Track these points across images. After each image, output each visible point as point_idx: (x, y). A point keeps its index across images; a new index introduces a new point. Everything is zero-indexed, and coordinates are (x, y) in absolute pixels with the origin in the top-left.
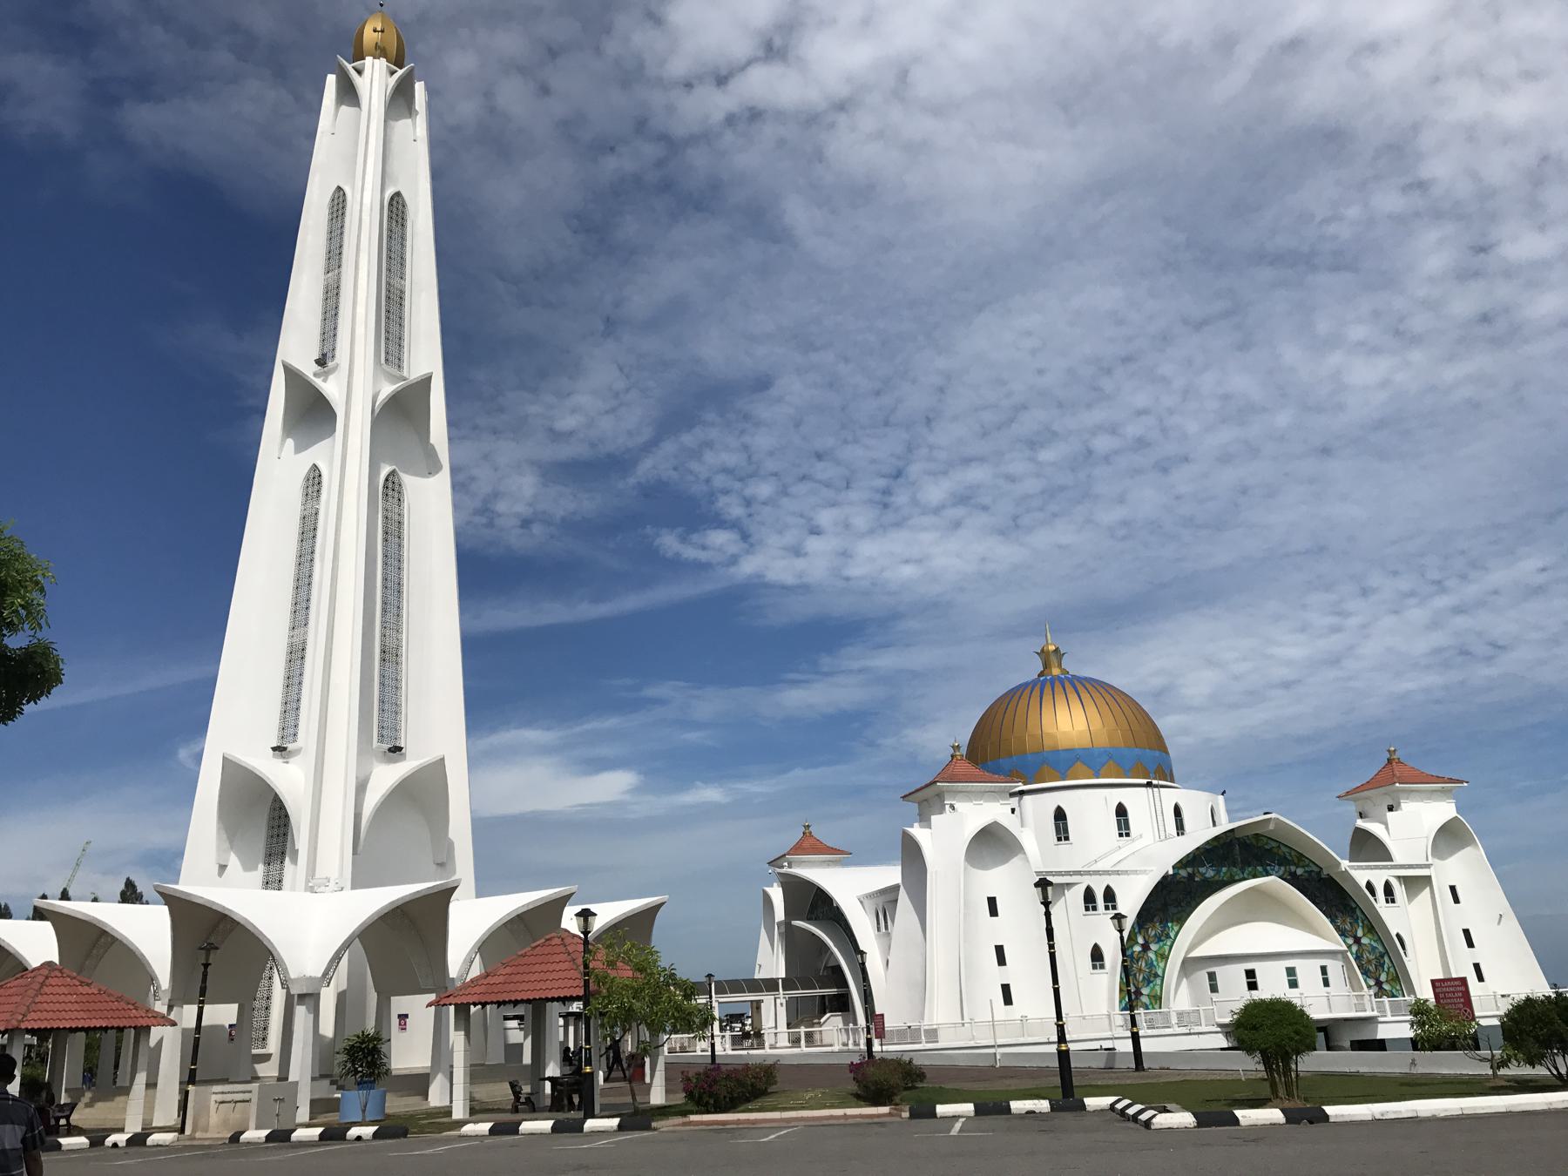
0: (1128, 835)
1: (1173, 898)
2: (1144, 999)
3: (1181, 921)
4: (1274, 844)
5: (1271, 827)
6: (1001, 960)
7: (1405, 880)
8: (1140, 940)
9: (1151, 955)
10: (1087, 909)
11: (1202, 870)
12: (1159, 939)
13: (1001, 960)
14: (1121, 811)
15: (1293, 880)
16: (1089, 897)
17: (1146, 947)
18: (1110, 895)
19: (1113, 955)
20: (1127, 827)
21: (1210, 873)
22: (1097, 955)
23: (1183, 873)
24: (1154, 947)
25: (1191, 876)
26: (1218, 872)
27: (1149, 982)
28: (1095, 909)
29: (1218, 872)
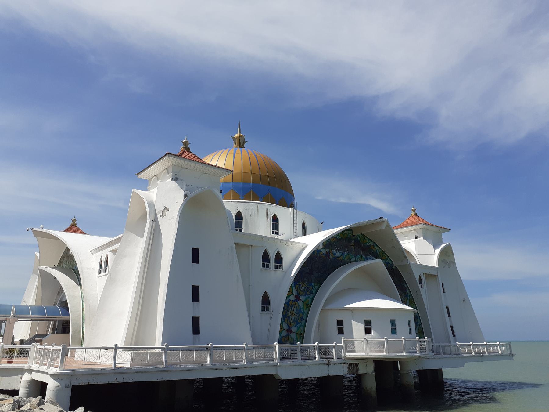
0: (277, 233)
1: (319, 266)
2: (293, 335)
3: (320, 281)
4: (371, 243)
5: (383, 227)
6: (196, 298)
7: (426, 275)
8: (295, 292)
9: (300, 303)
10: (263, 266)
11: (334, 251)
12: (306, 293)
13: (196, 298)
14: (275, 219)
15: (387, 265)
16: (266, 257)
17: (297, 298)
18: (279, 259)
19: (278, 302)
20: (277, 229)
21: (338, 254)
22: (266, 301)
23: (324, 251)
24: (302, 298)
25: (328, 254)
26: (342, 255)
27: (297, 323)
28: (268, 266)
29: (342, 255)
